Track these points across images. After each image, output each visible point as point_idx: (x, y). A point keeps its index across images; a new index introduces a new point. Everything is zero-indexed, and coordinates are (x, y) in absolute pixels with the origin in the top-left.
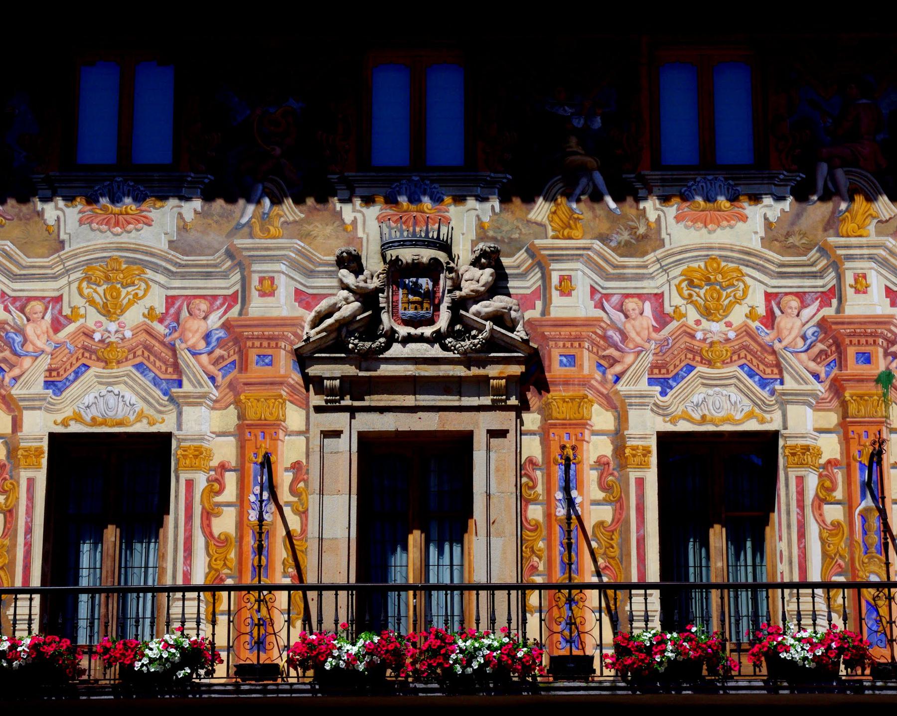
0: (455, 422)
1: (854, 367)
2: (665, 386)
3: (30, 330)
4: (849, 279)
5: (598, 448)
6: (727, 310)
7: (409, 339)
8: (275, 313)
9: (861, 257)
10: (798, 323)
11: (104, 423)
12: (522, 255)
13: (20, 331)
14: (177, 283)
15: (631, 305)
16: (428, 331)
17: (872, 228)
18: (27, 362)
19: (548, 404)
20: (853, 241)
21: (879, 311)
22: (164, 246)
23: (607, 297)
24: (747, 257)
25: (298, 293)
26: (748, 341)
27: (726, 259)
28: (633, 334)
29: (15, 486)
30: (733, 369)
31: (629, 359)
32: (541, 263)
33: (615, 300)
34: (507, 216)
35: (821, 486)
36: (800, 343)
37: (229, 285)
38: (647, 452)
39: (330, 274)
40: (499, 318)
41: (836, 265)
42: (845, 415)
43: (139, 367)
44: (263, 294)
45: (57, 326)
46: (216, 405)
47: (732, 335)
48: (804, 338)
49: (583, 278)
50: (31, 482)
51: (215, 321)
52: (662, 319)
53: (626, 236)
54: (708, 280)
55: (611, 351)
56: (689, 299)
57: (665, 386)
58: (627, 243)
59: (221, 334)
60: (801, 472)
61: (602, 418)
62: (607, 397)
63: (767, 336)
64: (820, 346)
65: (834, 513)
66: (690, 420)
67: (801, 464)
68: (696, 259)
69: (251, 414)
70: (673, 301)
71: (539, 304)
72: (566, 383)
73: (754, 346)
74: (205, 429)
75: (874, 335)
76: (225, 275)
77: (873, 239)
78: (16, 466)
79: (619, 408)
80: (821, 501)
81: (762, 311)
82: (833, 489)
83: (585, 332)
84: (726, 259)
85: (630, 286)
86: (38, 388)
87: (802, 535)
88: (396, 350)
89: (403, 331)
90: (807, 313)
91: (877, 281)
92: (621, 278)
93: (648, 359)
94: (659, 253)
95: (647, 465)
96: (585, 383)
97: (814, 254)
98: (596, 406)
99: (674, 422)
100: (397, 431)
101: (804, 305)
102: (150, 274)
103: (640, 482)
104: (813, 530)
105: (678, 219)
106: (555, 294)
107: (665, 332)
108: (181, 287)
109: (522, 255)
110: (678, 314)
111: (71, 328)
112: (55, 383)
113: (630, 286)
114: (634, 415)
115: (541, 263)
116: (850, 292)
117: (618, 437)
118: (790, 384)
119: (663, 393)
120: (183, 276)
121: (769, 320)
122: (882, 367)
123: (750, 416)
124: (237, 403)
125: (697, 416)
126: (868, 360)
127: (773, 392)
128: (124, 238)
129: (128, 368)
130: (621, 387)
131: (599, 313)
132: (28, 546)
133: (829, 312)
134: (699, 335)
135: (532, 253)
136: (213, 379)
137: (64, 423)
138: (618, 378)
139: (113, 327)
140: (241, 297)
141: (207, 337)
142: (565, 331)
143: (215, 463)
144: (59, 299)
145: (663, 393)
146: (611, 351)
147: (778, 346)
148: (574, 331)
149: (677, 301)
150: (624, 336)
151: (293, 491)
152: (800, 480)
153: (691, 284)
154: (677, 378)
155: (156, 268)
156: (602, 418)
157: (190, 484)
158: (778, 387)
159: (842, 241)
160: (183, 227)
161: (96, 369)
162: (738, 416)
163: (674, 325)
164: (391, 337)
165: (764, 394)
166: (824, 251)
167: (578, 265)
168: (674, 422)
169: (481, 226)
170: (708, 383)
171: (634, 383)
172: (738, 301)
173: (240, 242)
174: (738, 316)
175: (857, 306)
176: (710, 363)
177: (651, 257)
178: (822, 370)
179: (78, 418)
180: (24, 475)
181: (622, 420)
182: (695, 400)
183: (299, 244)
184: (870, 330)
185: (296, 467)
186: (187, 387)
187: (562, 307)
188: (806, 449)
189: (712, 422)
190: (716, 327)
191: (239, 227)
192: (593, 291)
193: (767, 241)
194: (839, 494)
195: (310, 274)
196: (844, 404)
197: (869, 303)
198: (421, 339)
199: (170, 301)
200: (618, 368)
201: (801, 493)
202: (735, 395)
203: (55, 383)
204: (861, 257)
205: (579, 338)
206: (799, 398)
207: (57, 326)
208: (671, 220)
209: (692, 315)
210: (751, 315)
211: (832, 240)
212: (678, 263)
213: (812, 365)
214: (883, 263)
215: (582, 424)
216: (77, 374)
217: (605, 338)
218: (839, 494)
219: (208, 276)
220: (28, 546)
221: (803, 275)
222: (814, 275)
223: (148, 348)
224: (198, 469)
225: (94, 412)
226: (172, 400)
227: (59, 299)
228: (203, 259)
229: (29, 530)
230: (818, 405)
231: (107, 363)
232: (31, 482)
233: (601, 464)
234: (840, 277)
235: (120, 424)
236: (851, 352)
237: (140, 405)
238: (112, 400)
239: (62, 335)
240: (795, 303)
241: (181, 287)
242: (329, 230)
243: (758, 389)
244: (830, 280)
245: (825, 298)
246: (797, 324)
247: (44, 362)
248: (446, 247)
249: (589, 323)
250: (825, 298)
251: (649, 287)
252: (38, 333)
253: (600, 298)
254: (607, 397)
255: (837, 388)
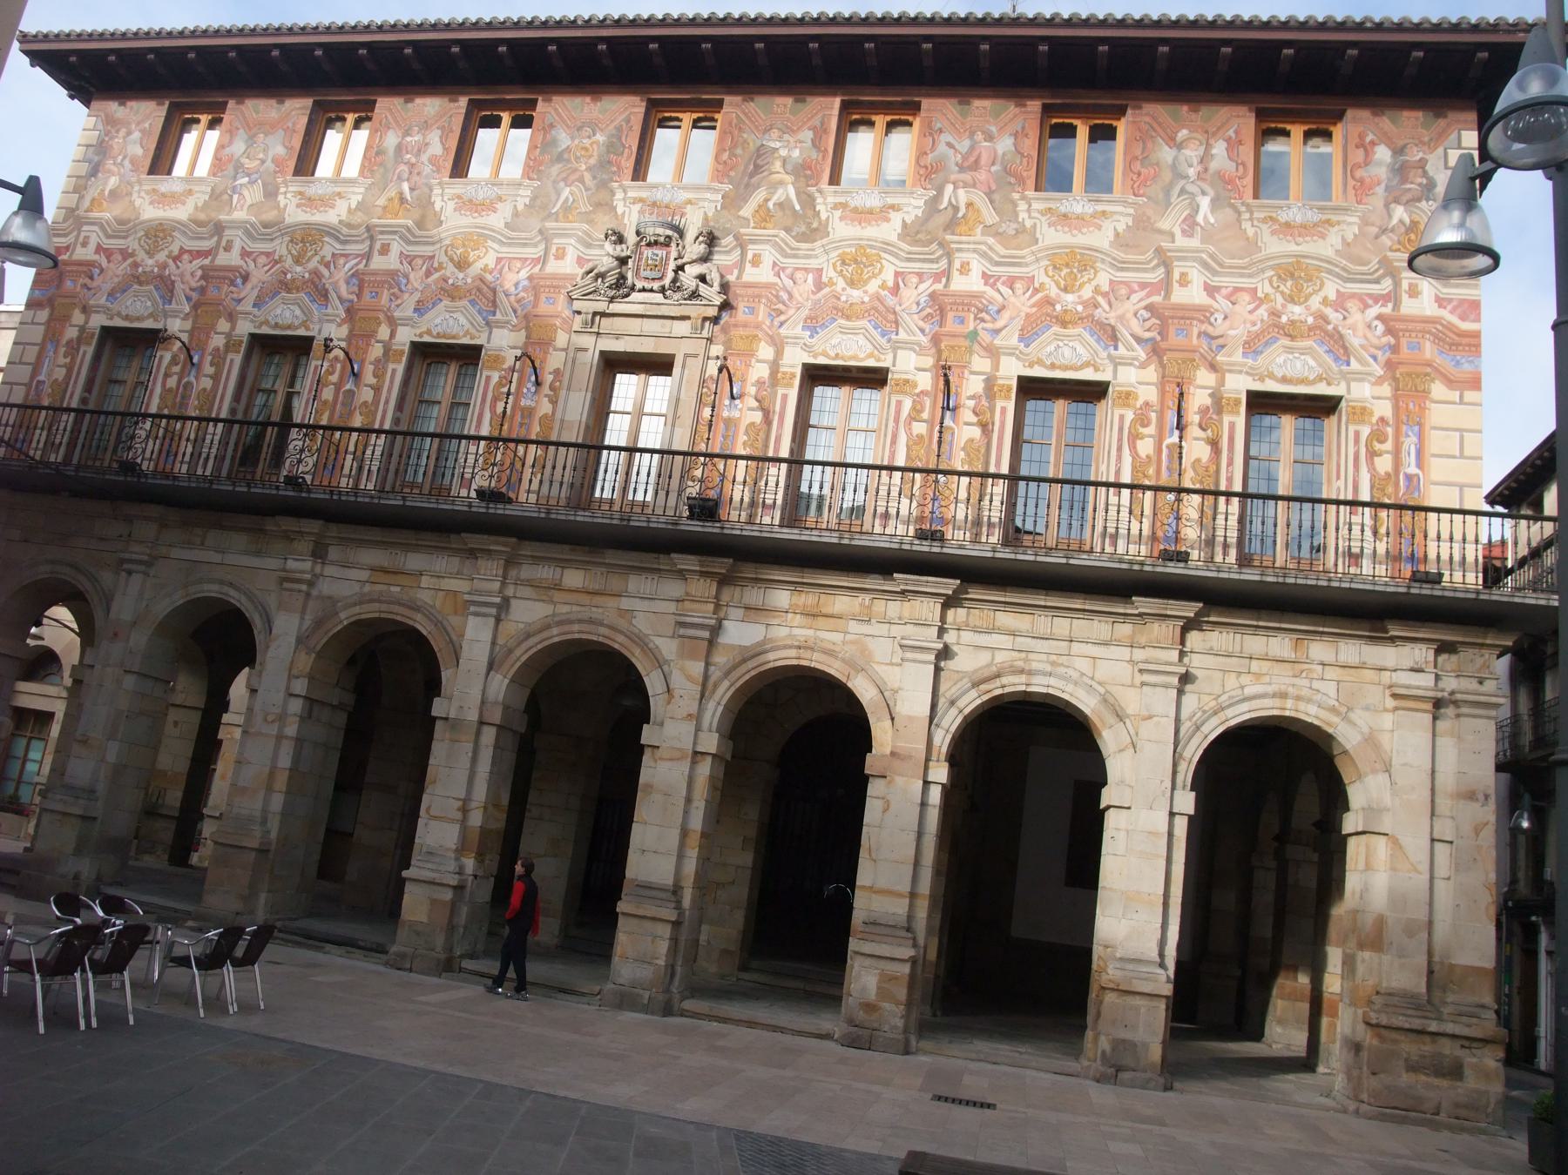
0: (663, 348)
1: (951, 325)
2: (814, 331)
3: (412, 276)
4: (957, 264)
5: (760, 371)
6: (866, 282)
7: (644, 290)
8: (562, 271)
9: (968, 250)
10: (916, 292)
11: (444, 336)
12: (730, 238)
13: (406, 276)
14: (505, 249)
15: (799, 275)
16: (656, 285)
17: (979, 230)
18: (406, 296)
19: (730, 340)
20: (964, 238)
21: (975, 288)
22: (502, 225)
23: (783, 269)
24: (887, 247)
25: (579, 258)
26: (877, 304)
27: (871, 247)
28: (796, 295)
29: (384, 374)
30: (864, 323)
31: (791, 312)
32: (742, 245)
33: (788, 271)
34: (725, 212)
35: (914, 408)
36: (914, 307)
37: (538, 251)
38: (793, 376)
39: (602, 247)
40: (702, 278)
41: (949, 255)
42: (939, 360)
43: (473, 302)
44: (557, 258)
45: (428, 274)
46: (515, 329)
47: (866, 299)
48: (918, 304)
49: (769, 255)
50: (394, 371)
51: (524, 274)
52: (819, 285)
53: (803, 228)
54: (856, 261)
55: (780, 306)
56: (841, 273)
57: (814, 331)
58: (804, 234)
59: (526, 283)
60: (900, 397)
61: (766, 351)
62: (771, 337)
63: (891, 301)
64: (929, 310)
65: (920, 428)
66: (827, 356)
67: (902, 392)
68: (850, 246)
69: (534, 336)
70: (829, 273)
71: (736, 272)
72: (745, 326)
73: (881, 308)
74: (504, 343)
75: (969, 305)
76: (535, 246)
77: (978, 238)
78: (387, 361)
79: (779, 346)
80: (912, 418)
81: (890, 284)
82: (922, 411)
83: (764, 292)
84: (871, 247)
85: (801, 262)
86: (409, 313)
87: (894, 442)
88: (635, 296)
89: (639, 285)
90: (922, 287)
91: (977, 266)
92: (795, 256)
93: (805, 312)
94: (825, 241)
95: (790, 385)
96: (758, 326)
97: (934, 246)
98: (763, 343)
99: (815, 357)
100: (625, 353)
101: (921, 281)
102: (490, 243)
103: (785, 397)
104: (903, 439)
105: (841, 219)
106: (748, 265)
107: (819, 295)
108: (506, 252)
109: (730, 238)
110: (831, 283)
111: (436, 275)
112: (420, 309)
113: (801, 262)
114: (788, 351)
115: (742, 245)
116: (955, 274)
117: (775, 366)
118: (902, 335)
119: (811, 336)
120: (510, 245)
121: (895, 290)
122: (971, 328)
123: (871, 355)
124: (527, 328)
125: (832, 354)
126: (962, 322)
127: (889, 341)
128: (480, 221)
129: (465, 302)
130: (783, 331)
131: (777, 280)
132: (385, 412)
133: (939, 287)
134: (843, 298)
135: (736, 238)
136: (515, 311)
137: (421, 335)
138: (782, 324)
139: (461, 276)
140: (543, 260)
141: (516, 285)
142: (750, 291)
143: (506, 366)
144: (432, 257)
145: (811, 336)
146: (780, 306)
147: (898, 308)
148: (757, 291)
149: (832, 274)
150: (791, 296)
151: (552, 388)
152: (899, 403)
153: (844, 263)
154: (823, 326)
155: (494, 239)
156: (766, 351)
157: (488, 378)
158: (893, 337)
159: (956, 238)
160: (516, 214)
161: (446, 302)
162: (862, 356)
163: (827, 290)
164: (633, 288)
165: (883, 341)
166: (941, 245)
167: (767, 247)
168: (815, 357)
169: (706, 219)
170: (844, 331)
171: (794, 329)
172: (874, 276)
173: (548, 224)
174: (873, 286)
175: (959, 284)
176: (848, 318)
177: (818, 243)
178: (927, 327)
179: (429, 332)
180: (391, 366)
181: (779, 353)
182: (833, 342)
183: (585, 226)
184: (968, 302)
185: (557, 372)
186: (498, 316)
187: (751, 274)
188: (907, 381)
189: (842, 358)
190: (856, 294)
191: (550, 215)
192: (775, 264)
193: (901, 237)
194: (925, 415)
195: (589, 246)
196: (939, 352)
197: (968, 283)
198: (651, 290)
199: (499, 260)
200: (782, 318)
201: (898, 413)
202: (862, 341)
203: (420, 309)
204: (968, 250)
205: (759, 296)
206: (907, 345)
207: (428, 274)
208: (836, 219)
209: (841, 283)
210: (883, 286)
211: (949, 237)
212: (837, 248)
213: (921, 323)
214: (984, 255)
215: (749, 354)
216: (434, 305)
217: (777, 297)
218: (925, 415)
219: (525, 245)
220: (385, 412)
221: (924, 261)
222: (931, 261)
223: (479, 290)
224: (495, 369)
225: (439, 329)
226: (488, 324)
227: (432, 257)
228: (523, 235)
229: (387, 402)
230: (921, 350)
231: (453, 299)
232: (394, 371)
233: (760, 383)
234: (950, 264)
235: (454, 337)
236: (950, 315)
237: (467, 326)
238: (451, 322)
239: (430, 280)
240: (915, 280)
241: (506, 252)
242: (606, 218)
243: (878, 337)
244: (943, 263)
245: (937, 277)
246: (915, 294)
247: (417, 296)
248: (681, 234)
249: (768, 286)
250: (937, 277)
251: (813, 263)
252: (416, 278)
253: (778, 269)
254: (771, 337)
255: (936, 340)
